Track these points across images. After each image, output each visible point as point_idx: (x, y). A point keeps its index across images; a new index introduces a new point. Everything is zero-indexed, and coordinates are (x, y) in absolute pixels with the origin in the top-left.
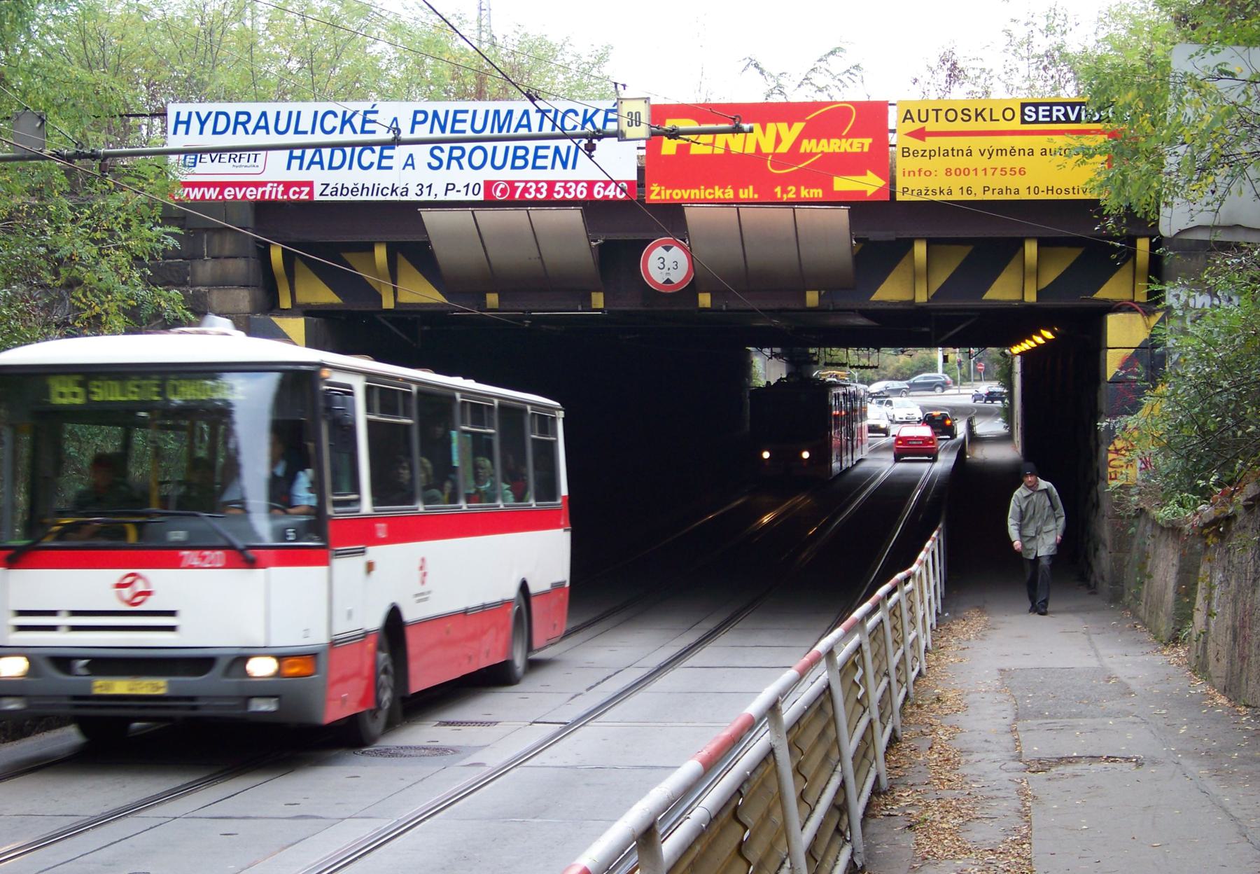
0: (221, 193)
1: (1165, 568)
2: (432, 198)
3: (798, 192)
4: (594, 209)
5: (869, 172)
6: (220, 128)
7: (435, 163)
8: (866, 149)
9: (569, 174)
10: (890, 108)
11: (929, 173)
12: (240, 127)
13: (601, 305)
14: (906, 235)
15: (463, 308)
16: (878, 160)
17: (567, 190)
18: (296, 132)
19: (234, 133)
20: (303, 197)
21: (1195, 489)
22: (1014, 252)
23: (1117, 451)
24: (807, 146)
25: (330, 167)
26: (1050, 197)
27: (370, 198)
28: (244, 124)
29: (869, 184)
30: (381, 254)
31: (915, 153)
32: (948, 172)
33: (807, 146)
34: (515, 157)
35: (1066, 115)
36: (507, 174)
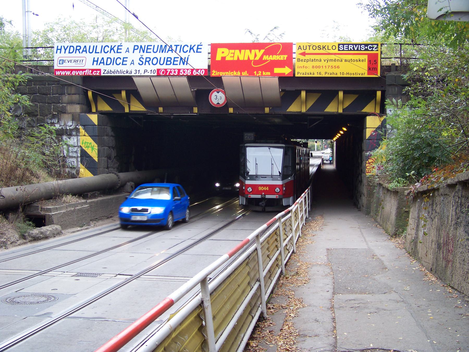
0: (71, 73)
1: (390, 206)
2: (139, 75)
3: (262, 73)
4: (193, 79)
5: (286, 67)
6: (71, 51)
7: (141, 63)
8: (285, 59)
9: (185, 67)
10: (294, 46)
12: (77, 51)
13: (197, 112)
14: (299, 88)
15: (152, 112)
16: (289, 63)
17: (184, 72)
18: (96, 52)
19: (76, 53)
20: (98, 74)
21: (406, 177)
22: (335, 96)
23: (369, 163)
24: (265, 58)
25: (107, 64)
26: (348, 76)
27: (119, 75)
28: (79, 50)
29: (286, 71)
30: (124, 94)
31: (302, 60)
32: (313, 67)
33: (265, 58)
34: (167, 61)
35: (353, 48)
36: (165, 67)
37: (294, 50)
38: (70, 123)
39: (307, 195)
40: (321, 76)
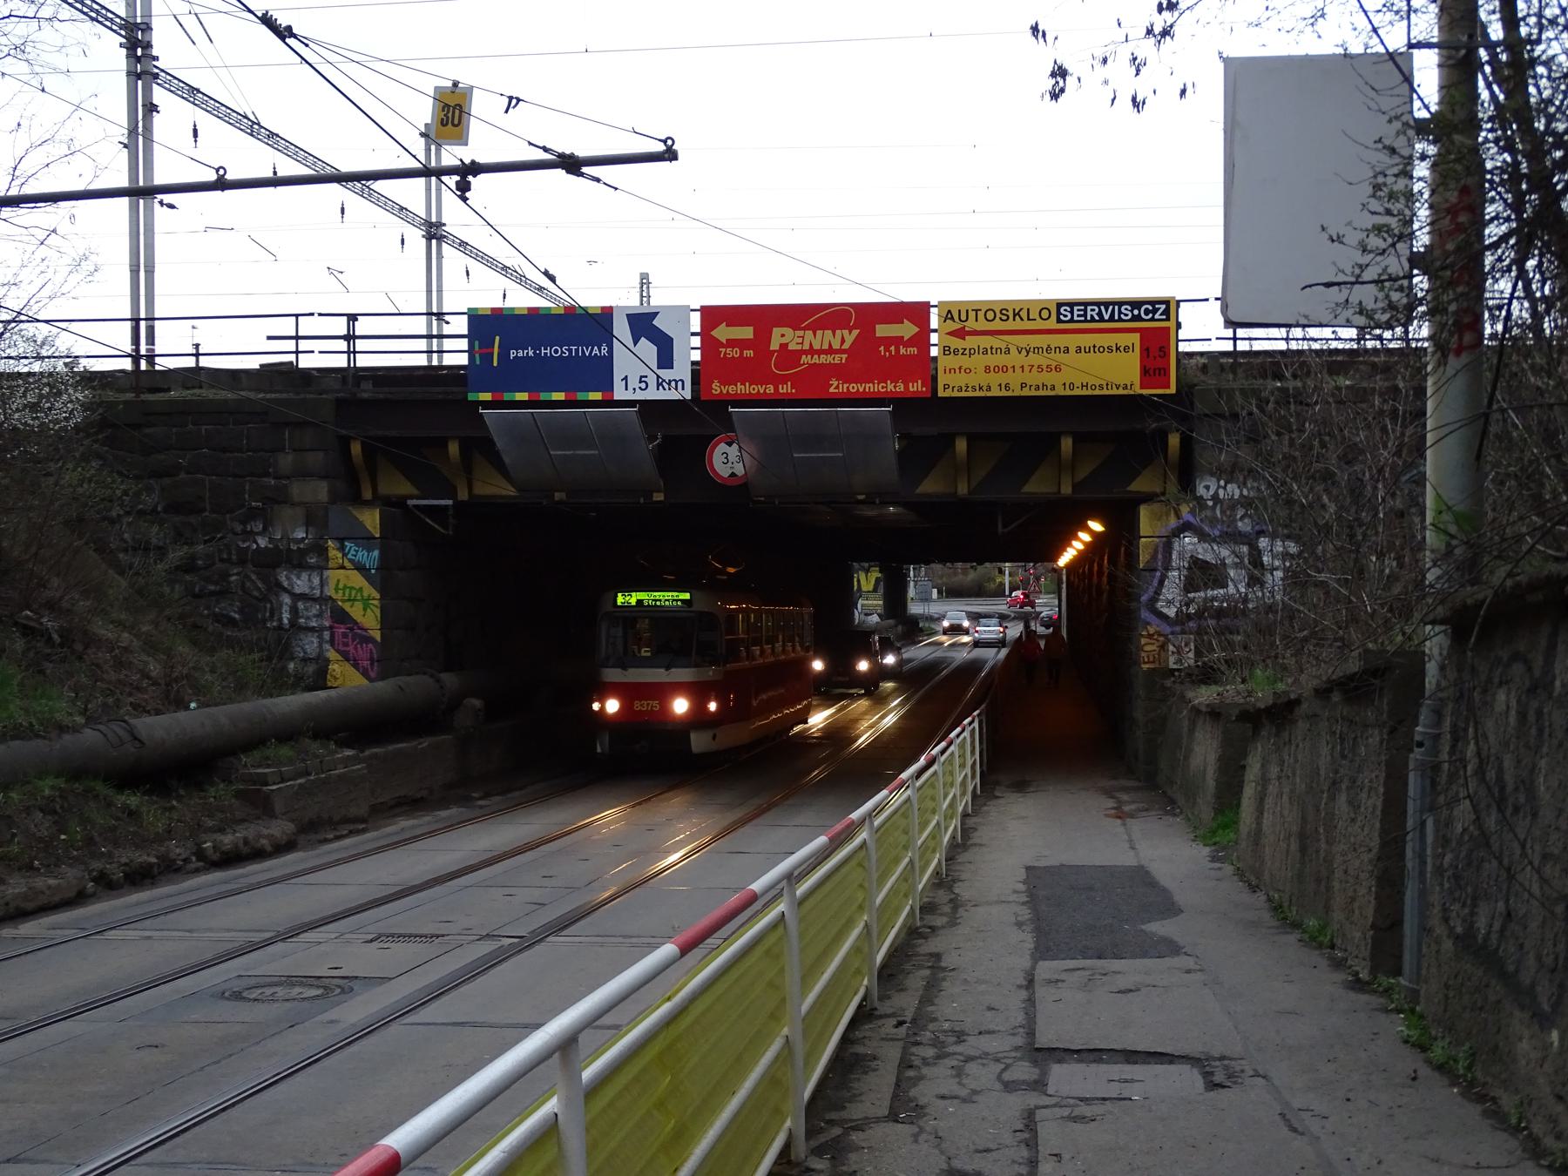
11: (968, 371)
23: (1150, 636)
30: (454, 448)
31: (956, 352)
37: (934, 324)
38: (300, 534)
39: (976, 724)
40: (1009, 394)
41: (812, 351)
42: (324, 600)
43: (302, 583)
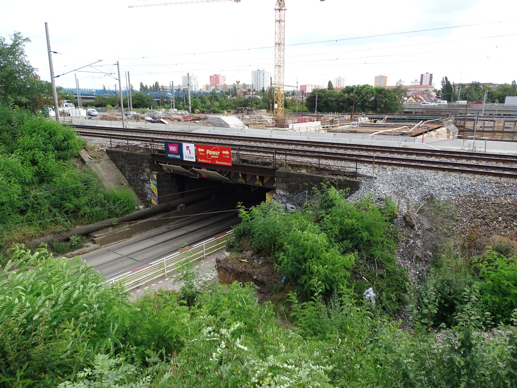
41: (213, 155)
42: (150, 189)
43: (147, 185)
